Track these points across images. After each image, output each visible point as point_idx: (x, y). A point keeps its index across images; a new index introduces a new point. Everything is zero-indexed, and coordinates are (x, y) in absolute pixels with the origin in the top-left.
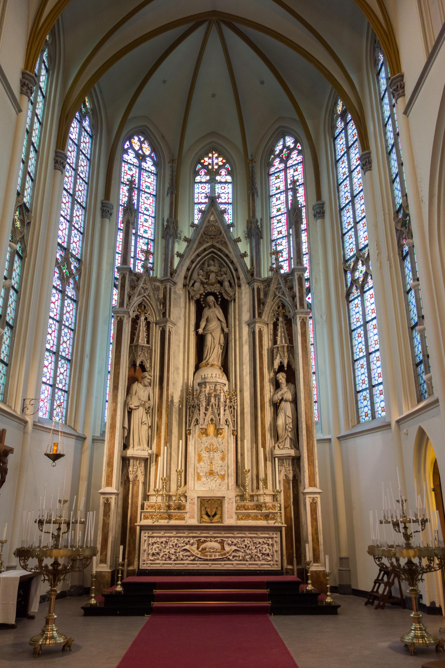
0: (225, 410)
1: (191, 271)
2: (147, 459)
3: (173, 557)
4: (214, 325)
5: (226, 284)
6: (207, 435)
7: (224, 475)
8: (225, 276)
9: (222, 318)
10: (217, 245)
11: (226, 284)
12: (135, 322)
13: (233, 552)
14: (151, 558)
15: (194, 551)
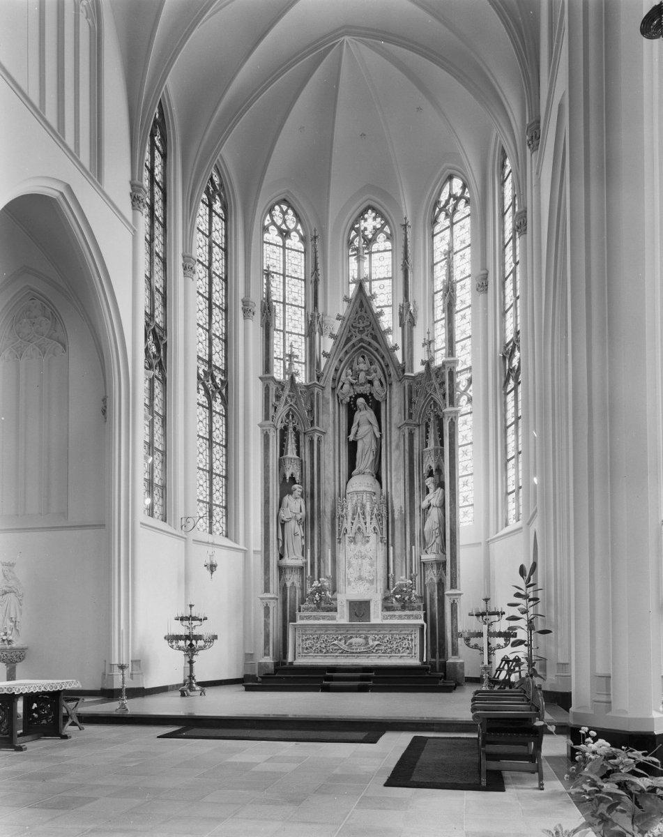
0: (371, 519)
1: (340, 371)
2: (303, 567)
3: (324, 651)
4: (364, 429)
5: (376, 383)
6: (355, 543)
7: (373, 579)
8: (374, 374)
9: (373, 420)
10: (366, 338)
11: (376, 383)
12: (284, 432)
13: (376, 646)
14: (305, 651)
15: (342, 645)
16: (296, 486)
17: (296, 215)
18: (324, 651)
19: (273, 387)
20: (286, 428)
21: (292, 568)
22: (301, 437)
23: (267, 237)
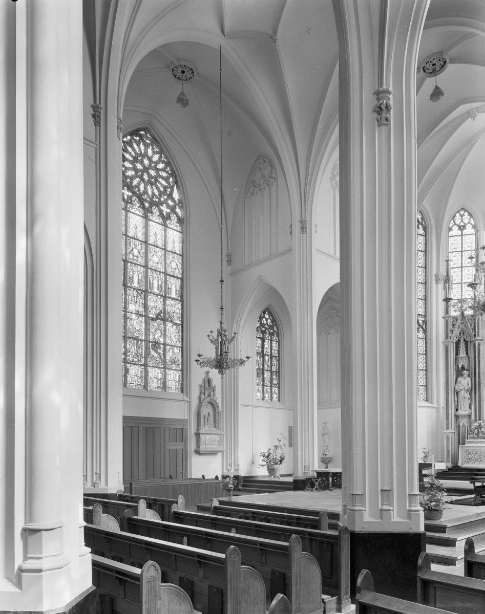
12: (458, 343)
16: (465, 372)
17: (470, 214)
18: (479, 460)
19: (451, 320)
20: (459, 341)
21: (463, 416)
22: (469, 343)
23: (451, 233)
